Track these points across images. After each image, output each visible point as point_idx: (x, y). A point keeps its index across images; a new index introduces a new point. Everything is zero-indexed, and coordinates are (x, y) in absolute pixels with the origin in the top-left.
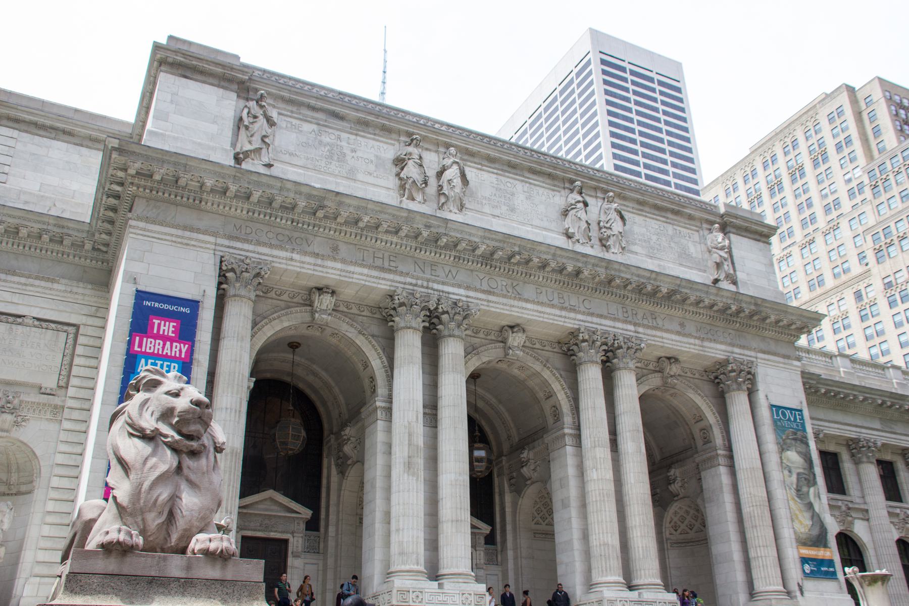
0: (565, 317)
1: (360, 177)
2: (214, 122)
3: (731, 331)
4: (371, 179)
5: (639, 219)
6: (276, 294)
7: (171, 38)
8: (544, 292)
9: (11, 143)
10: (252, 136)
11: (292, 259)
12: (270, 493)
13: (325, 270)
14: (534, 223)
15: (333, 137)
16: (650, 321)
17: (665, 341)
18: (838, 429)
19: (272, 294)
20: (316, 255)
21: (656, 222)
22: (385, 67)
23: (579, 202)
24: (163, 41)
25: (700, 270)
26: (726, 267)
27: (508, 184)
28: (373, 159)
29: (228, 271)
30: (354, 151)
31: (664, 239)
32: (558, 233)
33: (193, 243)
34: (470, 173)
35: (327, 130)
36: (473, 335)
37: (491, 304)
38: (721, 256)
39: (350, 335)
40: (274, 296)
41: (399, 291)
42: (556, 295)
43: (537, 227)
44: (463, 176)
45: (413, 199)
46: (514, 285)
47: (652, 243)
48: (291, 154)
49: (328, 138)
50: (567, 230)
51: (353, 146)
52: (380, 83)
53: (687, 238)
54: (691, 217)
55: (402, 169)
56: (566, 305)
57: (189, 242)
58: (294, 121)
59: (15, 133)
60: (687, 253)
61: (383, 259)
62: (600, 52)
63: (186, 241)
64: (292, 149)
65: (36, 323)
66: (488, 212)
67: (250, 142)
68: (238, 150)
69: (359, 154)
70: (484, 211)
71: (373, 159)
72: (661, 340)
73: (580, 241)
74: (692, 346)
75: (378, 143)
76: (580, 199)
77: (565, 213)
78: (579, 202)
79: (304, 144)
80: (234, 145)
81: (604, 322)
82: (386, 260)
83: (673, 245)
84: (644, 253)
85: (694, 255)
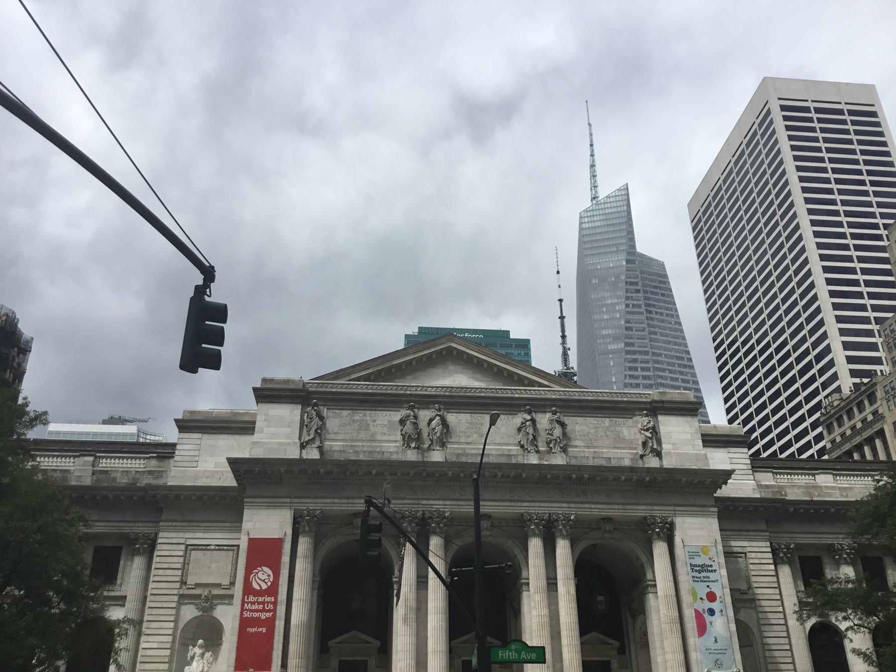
1: (379, 437)
2: (289, 427)
5: (579, 420)
7: (264, 380)
9: (198, 442)
10: (310, 431)
11: (334, 503)
12: (354, 633)
13: (354, 505)
14: (497, 442)
15: (361, 415)
17: (593, 510)
18: (815, 538)
20: (348, 498)
21: (595, 419)
22: (591, 141)
23: (528, 421)
24: (258, 385)
25: (630, 449)
26: (651, 444)
27: (479, 418)
28: (386, 423)
29: (298, 517)
30: (374, 421)
31: (601, 430)
32: (515, 445)
33: (279, 504)
34: (452, 418)
35: (357, 411)
37: (461, 507)
38: (646, 436)
44: (444, 423)
45: (409, 446)
47: (590, 435)
48: (336, 433)
49: (359, 416)
52: (589, 157)
53: (622, 425)
54: (625, 409)
55: (404, 427)
57: (276, 504)
58: (337, 411)
59: (199, 435)
60: (621, 436)
62: (779, 99)
63: (274, 504)
64: (336, 430)
65: (217, 548)
66: (464, 441)
67: (309, 435)
68: (302, 441)
69: (378, 422)
70: (461, 441)
71: (386, 423)
72: (590, 510)
73: (529, 449)
74: (616, 511)
75: (390, 412)
76: (529, 417)
77: (519, 430)
78: (528, 421)
80: (300, 439)
84: (583, 444)
85: (627, 438)
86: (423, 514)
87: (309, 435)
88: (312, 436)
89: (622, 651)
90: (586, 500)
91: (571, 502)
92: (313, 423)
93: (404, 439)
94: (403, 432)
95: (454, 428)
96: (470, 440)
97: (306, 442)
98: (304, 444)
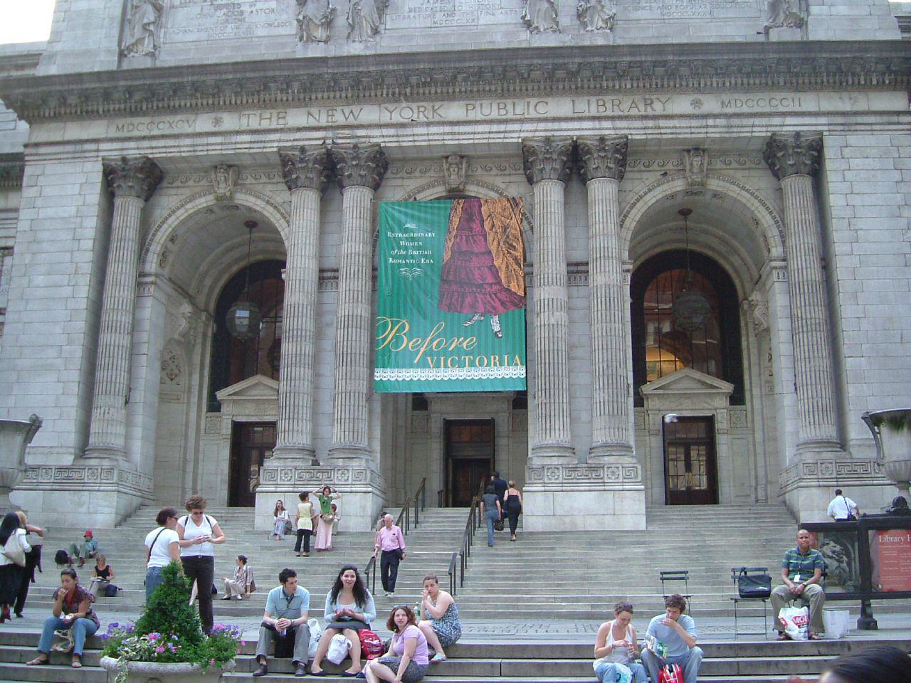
0: (505, 132)
3: (783, 95)
6: (181, 182)
8: (478, 108)
16: (641, 107)
19: (178, 183)
36: (405, 175)
39: (258, 208)
40: (180, 184)
42: (495, 107)
46: (436, 108)
50: (523, 18)
56: (510, 116)
61: (270, 118)
79: (198, 16)
80: (119, 45)
81: (564, 125)
82: (274, 119)
87: (133, 36)
88: (137, 36)
89: (737, 398)
90: (650, 112)
91: (620, 118)
92: (137, 16)
93: (301, 26)
94: (301, 17)
97: (128, 48)
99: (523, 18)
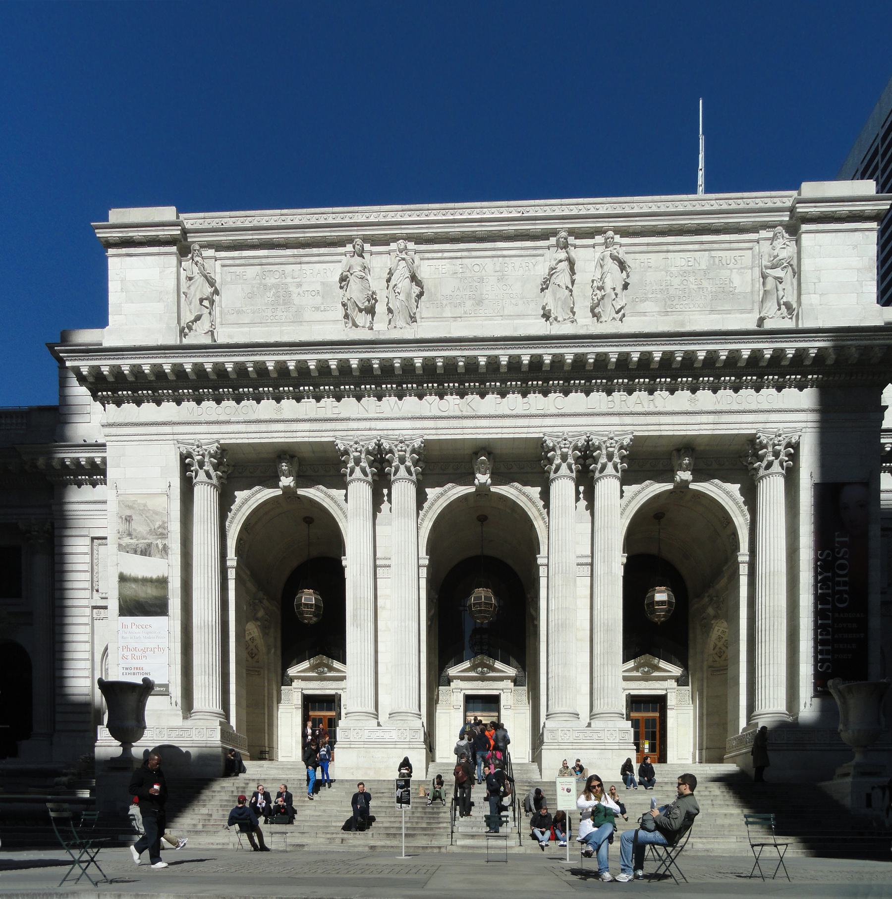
4: (318, 316)
14: (506, 312)
16: (646, 404)
17: (663, 427)
25: (742, 311)
27: (476, 268)
28: (319, 287)
30: (299, 285)
34: (426, 270)
41: (338, 441)
43: (510, 316)
51: (298, 280)
66: (450, 315)
69: (305, 287)
70: (444, 315)
71: (319, 287)
72: (657, 427)
83: (705, 283)
86: (379, 445)
95: (433, 290)
96: (459, 312)
98: (186, 330)
99: (544, 308)
